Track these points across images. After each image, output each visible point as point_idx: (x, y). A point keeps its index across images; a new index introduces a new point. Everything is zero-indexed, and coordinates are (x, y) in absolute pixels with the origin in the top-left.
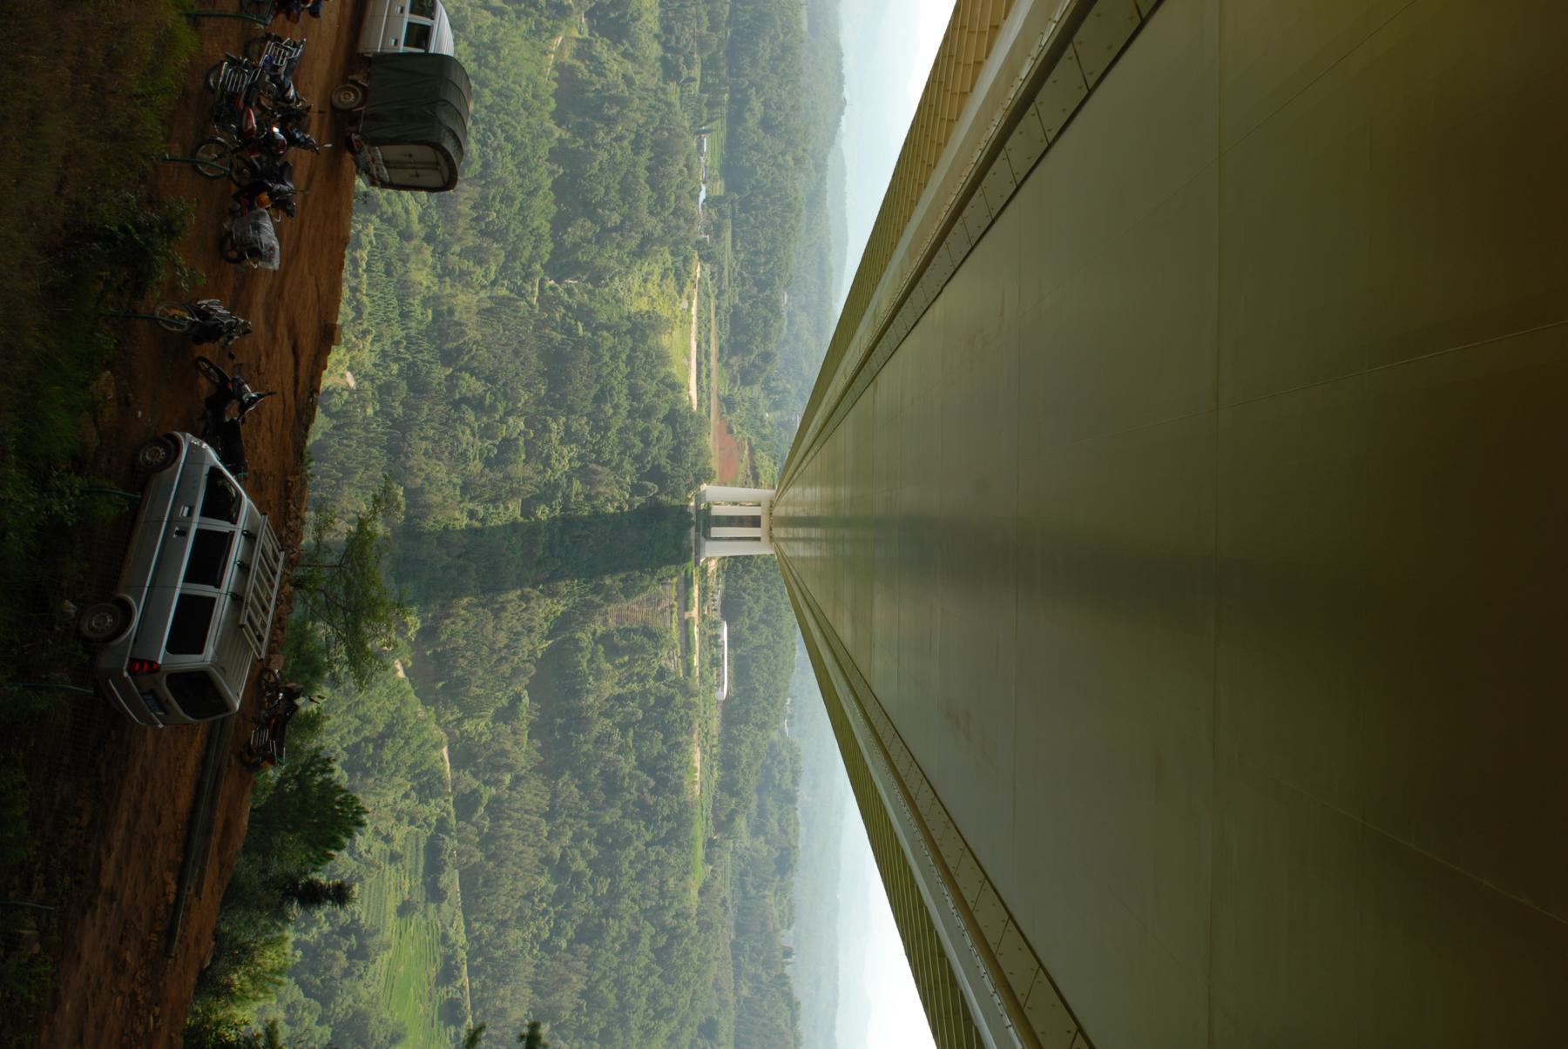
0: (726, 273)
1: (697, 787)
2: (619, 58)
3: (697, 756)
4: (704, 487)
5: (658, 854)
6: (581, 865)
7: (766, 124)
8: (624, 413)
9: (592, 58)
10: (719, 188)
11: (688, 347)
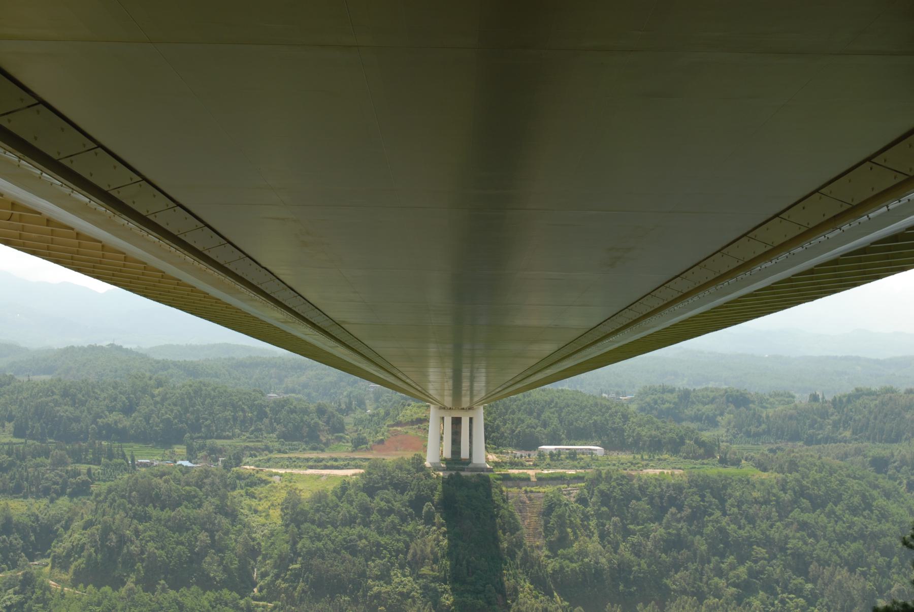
0: (251, 444)
1: (677, 472)
2: (69, 532)
3: (651, 472)
4: (427, 464)
5: (732, 506)
6: (742, 570)
7: (128, 410)
8: (366, 530)
9: (69, 555)
10: (180, 449)
11: (311, 476)
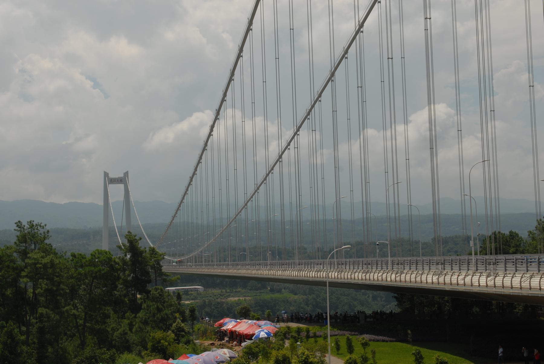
1: (247, 298)
